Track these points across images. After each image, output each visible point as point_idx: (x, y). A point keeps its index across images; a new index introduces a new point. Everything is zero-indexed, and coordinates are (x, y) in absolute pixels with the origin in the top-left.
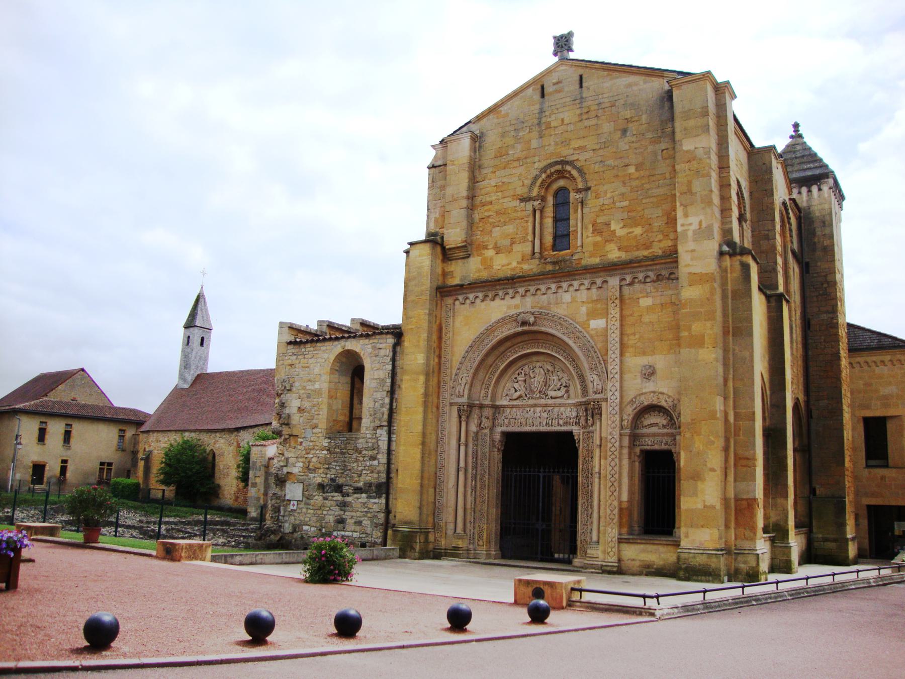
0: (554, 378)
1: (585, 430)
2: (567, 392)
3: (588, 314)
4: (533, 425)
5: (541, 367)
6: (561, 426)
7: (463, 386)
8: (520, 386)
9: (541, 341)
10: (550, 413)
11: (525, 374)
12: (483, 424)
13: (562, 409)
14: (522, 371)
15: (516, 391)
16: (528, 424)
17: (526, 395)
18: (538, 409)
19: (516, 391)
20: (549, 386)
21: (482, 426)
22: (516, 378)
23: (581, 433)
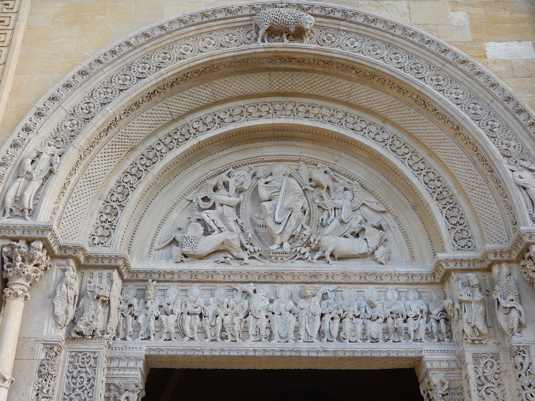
0: (339, 202)
1: (481, 350)
2: (383, 242)
3: (474, 28)
4: (270, 337)
5: (290, 176)
6: (375, 340)
7: (35, 185)
8: (222, 216)
9: (304, 100)
10: (329, 301)
11: (240, 191)
12: (86, 318)
13: (371, 292)
14: (231, 181)
15: (207, 232)
16: (252, 331)
17: (242, 246)
18: (283, 290)
19: (207, 232)
20: (323, 225)
21: (81, 326)
22: (205, 199)
23: (469, 358)
